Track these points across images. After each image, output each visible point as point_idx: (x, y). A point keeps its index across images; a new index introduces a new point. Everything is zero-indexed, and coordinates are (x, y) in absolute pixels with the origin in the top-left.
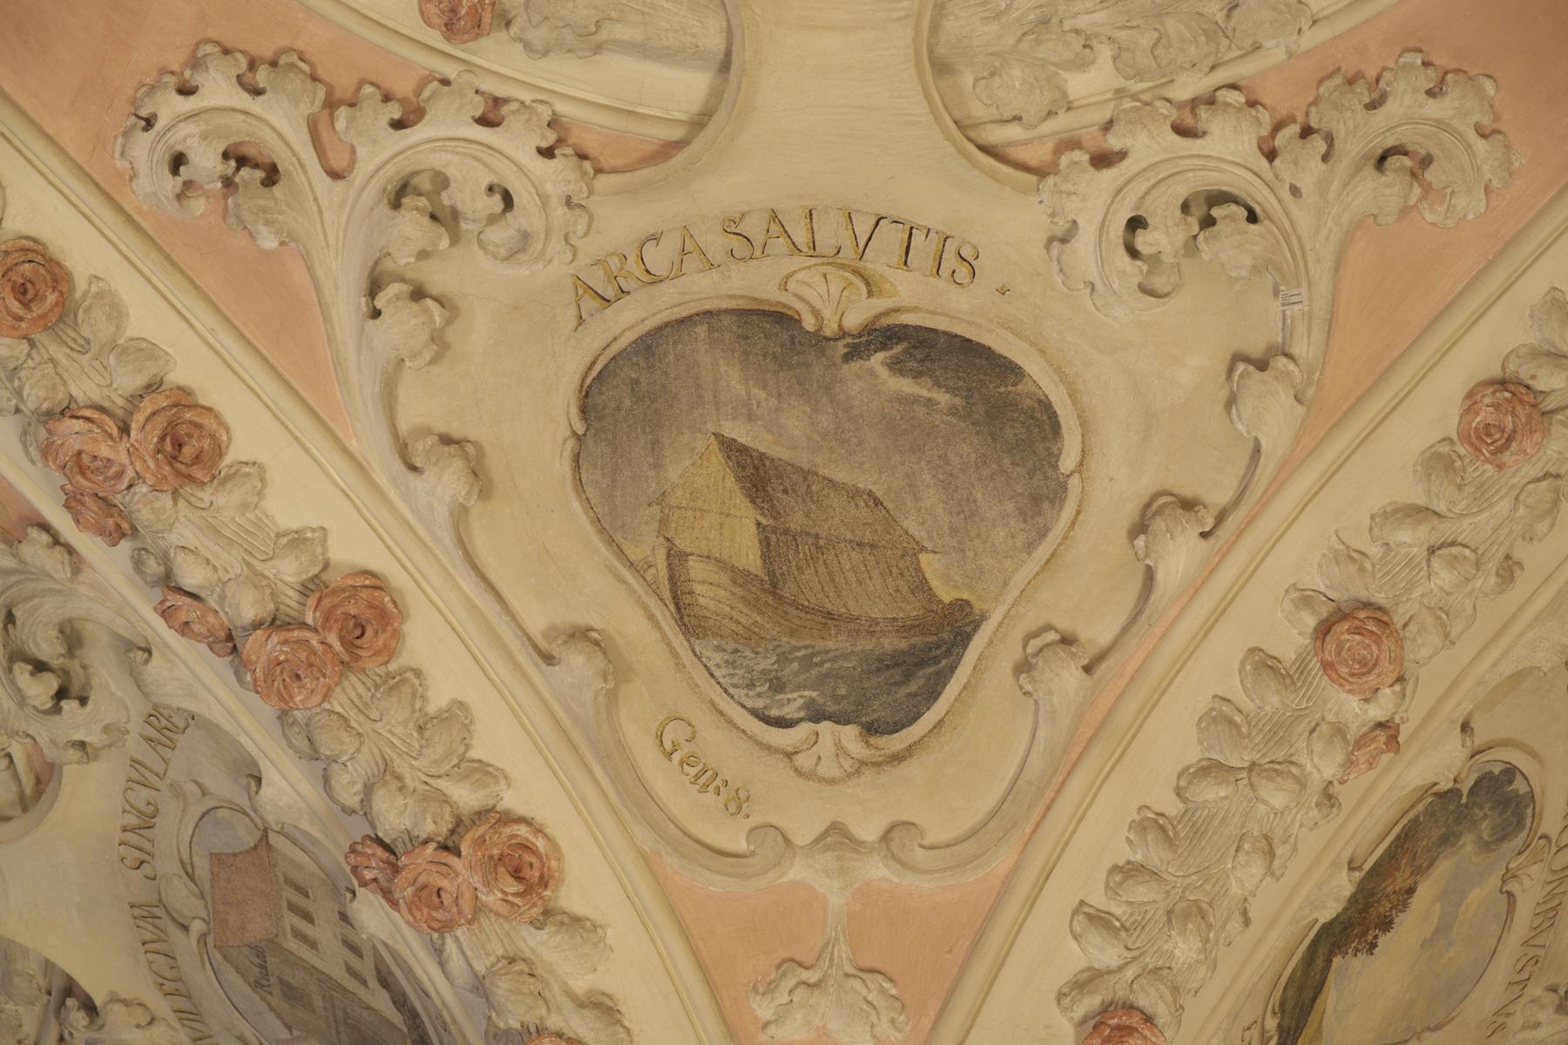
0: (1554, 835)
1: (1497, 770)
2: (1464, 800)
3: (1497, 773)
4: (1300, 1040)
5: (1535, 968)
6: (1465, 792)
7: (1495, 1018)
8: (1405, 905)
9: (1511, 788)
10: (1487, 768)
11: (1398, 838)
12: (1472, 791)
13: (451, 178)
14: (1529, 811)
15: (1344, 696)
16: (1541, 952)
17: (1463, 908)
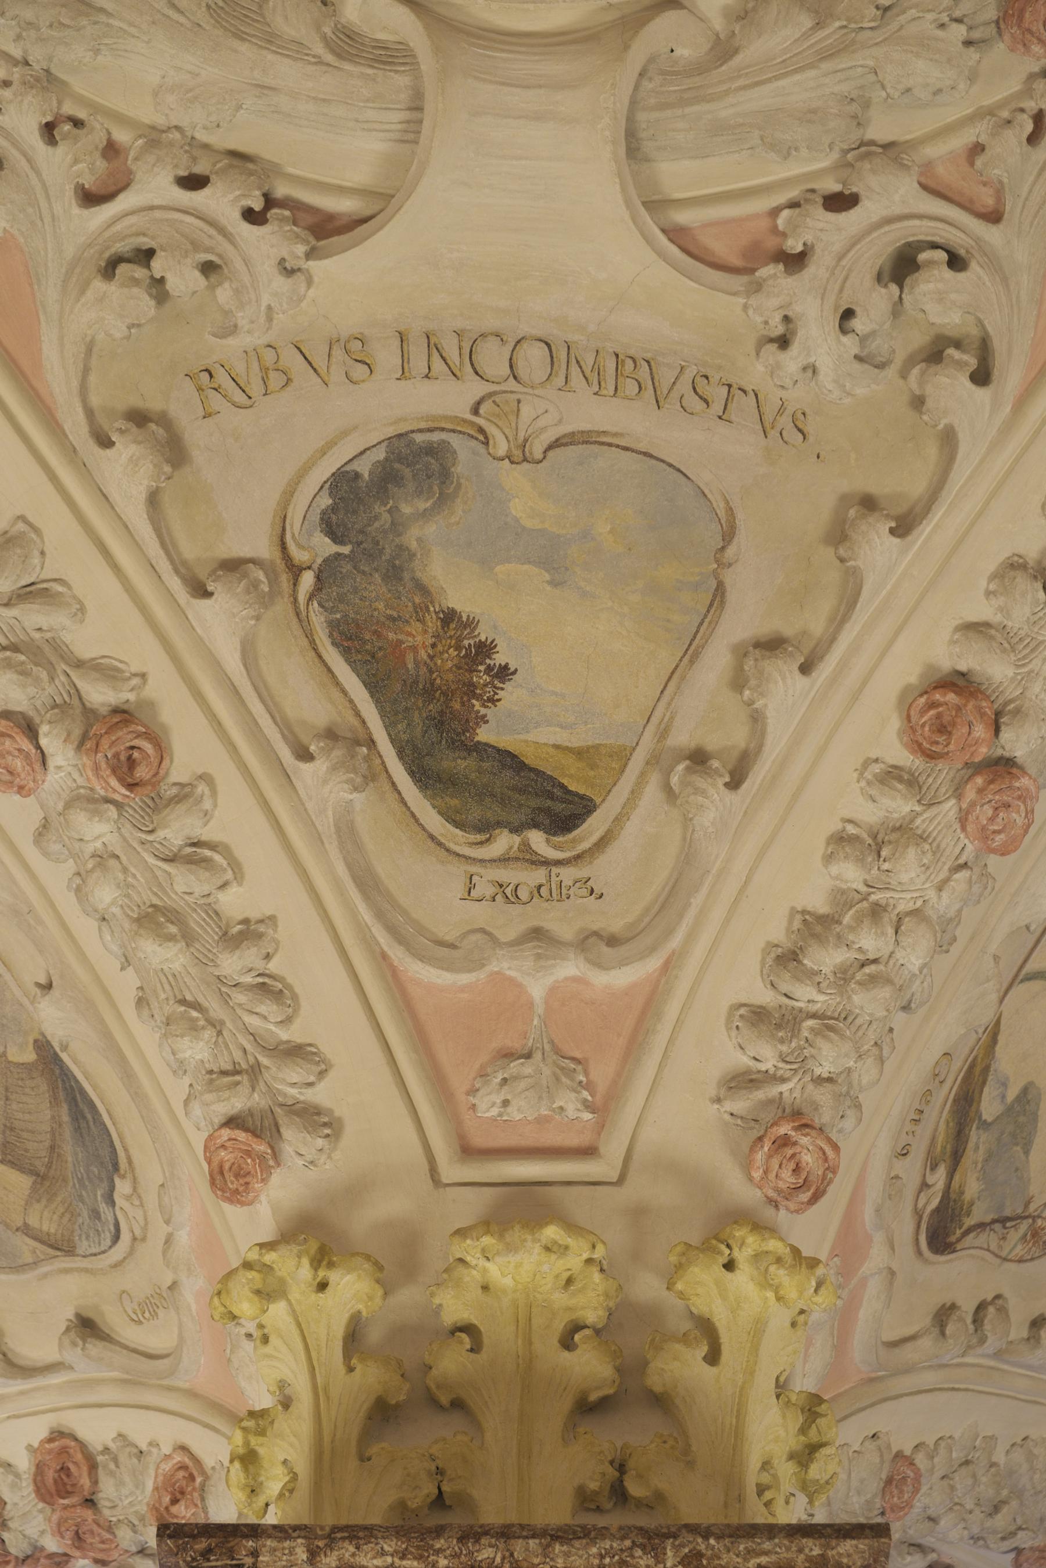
0: (476, 389)
1: (325, 501)
2: (346, 550)
3: (330, 501)
4: (572, 788)
5: (715, 378)
6: (335, 548)
7: (774, 434)
8: (471, 624)
9: (366, 476)
10: (315, 517)
11: (346, 653)
12: (337, 539)
13: (910, 538)
14: (419, 438)
15: (46, 785)
16: (691, 372)
17: (528, 523)
